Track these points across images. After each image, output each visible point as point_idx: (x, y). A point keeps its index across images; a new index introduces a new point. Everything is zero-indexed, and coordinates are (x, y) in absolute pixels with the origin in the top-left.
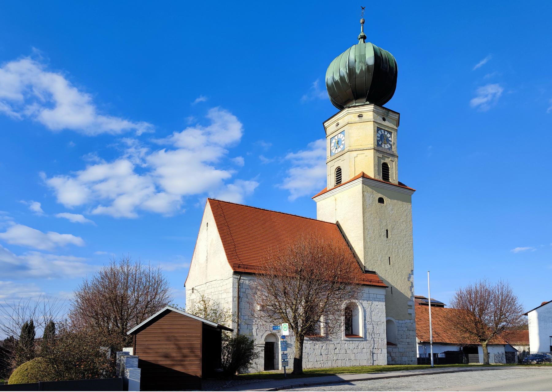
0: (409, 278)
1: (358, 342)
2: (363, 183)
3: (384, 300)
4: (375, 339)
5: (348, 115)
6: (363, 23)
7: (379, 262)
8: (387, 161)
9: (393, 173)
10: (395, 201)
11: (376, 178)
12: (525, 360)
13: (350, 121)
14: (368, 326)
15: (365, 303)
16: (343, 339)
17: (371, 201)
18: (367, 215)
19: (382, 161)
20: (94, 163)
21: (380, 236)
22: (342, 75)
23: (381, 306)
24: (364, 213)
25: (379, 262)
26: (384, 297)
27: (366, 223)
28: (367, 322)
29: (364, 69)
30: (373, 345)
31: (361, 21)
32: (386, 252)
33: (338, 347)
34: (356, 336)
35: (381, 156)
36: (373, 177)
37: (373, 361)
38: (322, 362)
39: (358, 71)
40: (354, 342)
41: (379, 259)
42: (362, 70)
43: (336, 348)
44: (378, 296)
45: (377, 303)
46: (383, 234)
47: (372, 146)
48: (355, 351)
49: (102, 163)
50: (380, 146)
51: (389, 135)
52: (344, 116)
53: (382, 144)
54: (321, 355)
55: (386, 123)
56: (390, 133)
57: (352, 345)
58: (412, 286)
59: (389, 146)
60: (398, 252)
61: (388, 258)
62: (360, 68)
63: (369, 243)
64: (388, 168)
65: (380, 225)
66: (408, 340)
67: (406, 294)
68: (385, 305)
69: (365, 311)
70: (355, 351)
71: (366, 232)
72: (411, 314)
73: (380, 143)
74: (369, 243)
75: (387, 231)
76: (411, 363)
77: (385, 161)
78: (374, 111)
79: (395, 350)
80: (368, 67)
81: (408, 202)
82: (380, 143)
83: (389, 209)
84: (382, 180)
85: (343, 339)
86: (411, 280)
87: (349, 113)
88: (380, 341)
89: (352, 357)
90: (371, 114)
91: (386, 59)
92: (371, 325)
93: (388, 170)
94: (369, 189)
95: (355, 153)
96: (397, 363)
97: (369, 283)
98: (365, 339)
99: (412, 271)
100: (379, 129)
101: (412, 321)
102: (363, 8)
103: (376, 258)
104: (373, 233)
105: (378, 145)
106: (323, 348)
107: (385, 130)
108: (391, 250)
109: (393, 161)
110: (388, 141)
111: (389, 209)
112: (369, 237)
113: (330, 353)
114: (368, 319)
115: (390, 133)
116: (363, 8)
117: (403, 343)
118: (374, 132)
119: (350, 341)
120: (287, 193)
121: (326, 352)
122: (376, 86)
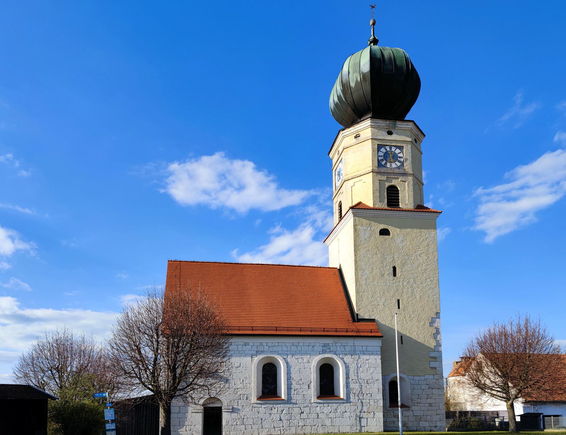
0: (432, 323)
1: (337, 405)
2: (355, 215)
3: (379, 353)
4: (364, 401)
5: (346, 138)
6: (374, 24)
7: (381, 307)
8: (394, 182)
9: (405, 196)
10: (409, 230)
11: (377, 206)
12: (554, 416)
13: (346, 146)
14: (352, 386)
15: (348, 359)
16: (313, 401)
17: (367, 234)
18: (362, 252)
19: (387, 184)
20: (278, 235)
21: (383, 275)
22: (339, 94)
23: (376, 360)
24: (355, 251)
25: (381, 307)
26: (379, 349)
27: (359, 263)
28: (350, 380)
29: (359, 80)
30: (360, 408)
31: (371, 23)
32: (392, 294)
33: (307, 410)
34: (338, 397)
35: (384, 178)
36: (371, 205)
37: (361, 427)
38: (281, 428)
39: (353, 84)
40: (330, 405)
41: (381, 303)
42: (357, 82)
43: (302, 413)
44: (370, 349)
45: (367, 357)
46: (387, 273)
47: (370, 169)
48: (331, 415)
49: (284, 234)
50: (385, 166)
51: (398, 151)
52: (341, 142)
53: (386, 163)
54: (281, 420)
55: (394, 137)
56: (401, 148)
57: (327, 408)
58: (438, 332)
59: (399, 164)
60: (412, 292)
61: (395, 302)
62: (355, 79)
63: (364, 286)
64: (398, 191)
65: (382, 262)
66: (429, 401)
67: (426, 344)
68: (382, 359)
69: (347, 367)
70: (331, 415)
71: (360, 273)
72: (435, 368)
73: (383, 163)
74: (364, 286)
75: (394, 268)
76: (434, 429)
77: (393, 184)
78: (372, 126)
79: (410, 413)
80: (364, 75)
81: (428, 228)
82: (383, 163)
83: (398, 241)
84: (386, 207)
85: (313, 401)
86: (436, 325)
87: (344, 137)
88: (372, 403)
89: (328, 422)
90: (369, 130)
91: (390, 58)
92: (358, 384)
93: (398, 193)
94: (365, 221)
95: (351, 182)
96: (411, 429)
97: (313, 333)
98: (348, 400)
99: (438, 314)
100: (380, 147)
101: (436, 377)
102: (373, 7)
103: (376, 303)
104: (371, 272)
105: (380, 165)
106: (284, 412)
107: (391, 147)
108: (400, 290)
109: (405, 182)
110: (395, 157)
111: (398, 241)
112: (364, 278)
113: (293, 418)
114: (352, 376)
115: (401, 148)
116: (373, 7)
117: (421, 405)
118: (373, 151)
119: (324, 403)
120: (483, 234)
121: (287, 417)
122: (389, 94)
